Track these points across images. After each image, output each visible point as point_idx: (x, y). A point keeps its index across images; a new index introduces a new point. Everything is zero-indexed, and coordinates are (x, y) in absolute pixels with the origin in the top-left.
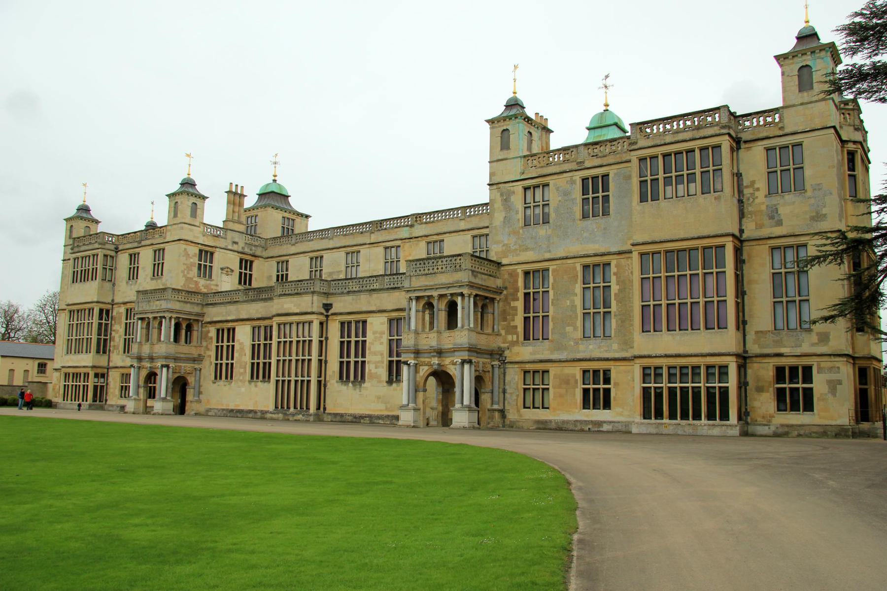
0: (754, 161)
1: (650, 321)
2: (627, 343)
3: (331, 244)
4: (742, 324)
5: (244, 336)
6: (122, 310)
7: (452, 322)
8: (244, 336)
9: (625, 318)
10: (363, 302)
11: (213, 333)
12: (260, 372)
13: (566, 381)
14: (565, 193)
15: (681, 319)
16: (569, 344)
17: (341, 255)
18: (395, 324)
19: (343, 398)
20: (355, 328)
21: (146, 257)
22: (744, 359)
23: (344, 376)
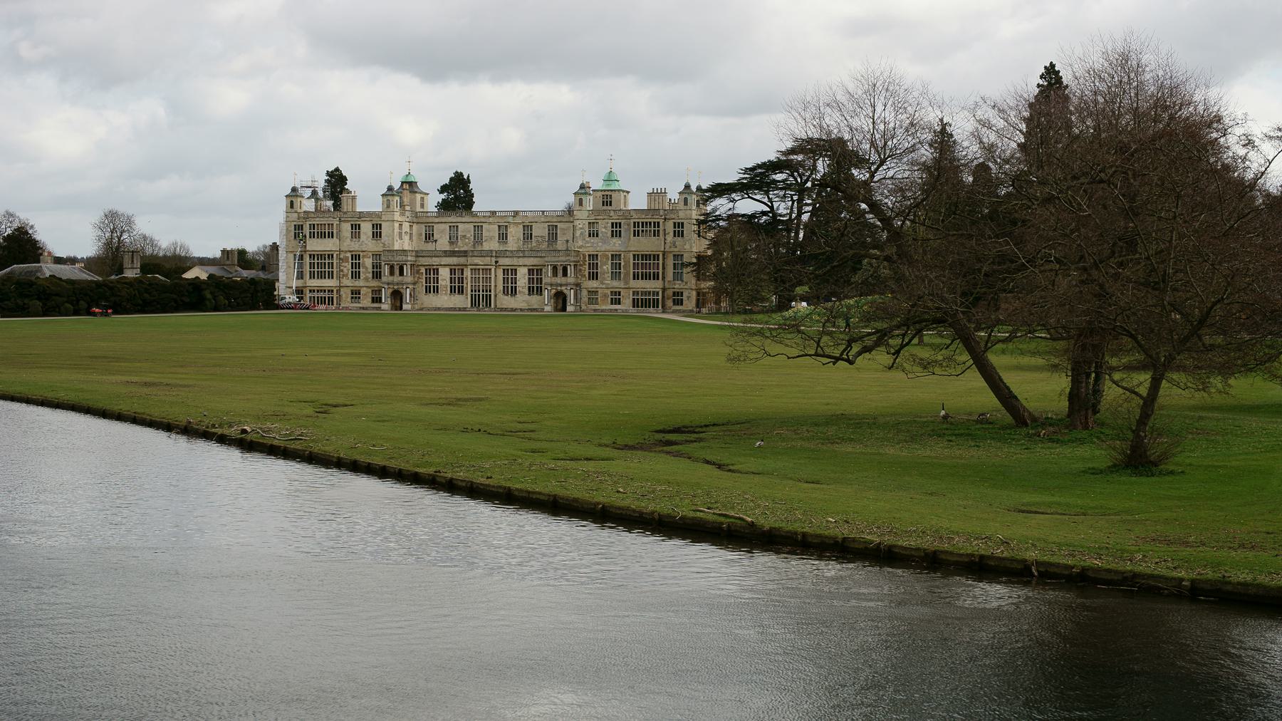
0: (670, 226)
1: (636, 277)
2: (627, 283)
3: (464, 220)
4: (664, 278)
5: (444, 274)
6: (349, 255)
7: (565, 274)
8: (444, 274)
9: (627, 274)
10: (515, 261)
11: (423, 270)
12: (457, 289)
13: (605, 295)
14: (604, 228)
15: (646, 277)
16: (606, 283)
17: (471, 226)
18: (535, 272)
19: (507, 302)
20: (510, 272)
21: (366, 228)
22: (664, 290)
23: (505, 292)
